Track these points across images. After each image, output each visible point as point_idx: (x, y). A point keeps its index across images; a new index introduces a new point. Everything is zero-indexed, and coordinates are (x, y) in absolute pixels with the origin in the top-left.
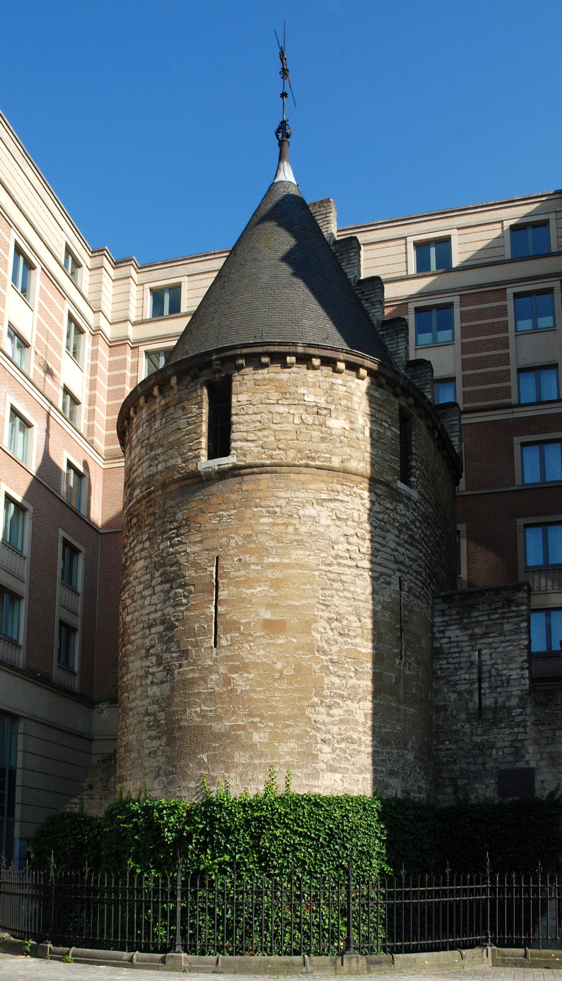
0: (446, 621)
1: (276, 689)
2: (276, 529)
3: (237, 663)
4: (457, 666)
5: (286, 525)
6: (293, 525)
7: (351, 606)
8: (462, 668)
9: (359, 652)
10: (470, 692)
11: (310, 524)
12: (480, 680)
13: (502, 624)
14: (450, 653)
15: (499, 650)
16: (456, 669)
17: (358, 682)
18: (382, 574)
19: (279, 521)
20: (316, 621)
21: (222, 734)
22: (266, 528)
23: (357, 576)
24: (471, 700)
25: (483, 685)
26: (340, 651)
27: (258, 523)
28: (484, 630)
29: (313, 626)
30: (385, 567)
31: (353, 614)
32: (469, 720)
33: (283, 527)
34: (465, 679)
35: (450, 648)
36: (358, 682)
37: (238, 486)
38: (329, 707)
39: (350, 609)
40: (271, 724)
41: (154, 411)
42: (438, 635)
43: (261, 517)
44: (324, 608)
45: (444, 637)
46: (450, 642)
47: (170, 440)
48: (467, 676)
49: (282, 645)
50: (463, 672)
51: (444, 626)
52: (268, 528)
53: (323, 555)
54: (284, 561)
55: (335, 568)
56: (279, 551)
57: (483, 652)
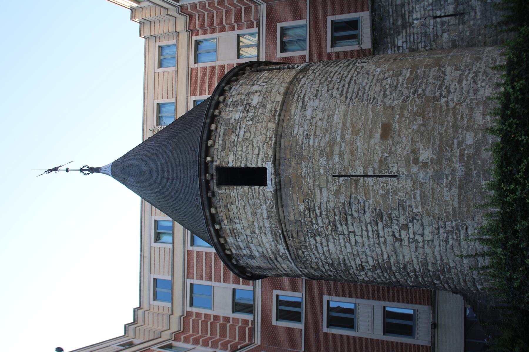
0: (391, 46)
1: (433, 129)
2: (318, 133)
3: (412, 158)
4: (423, 35)
5: (316, 126)
6: (317, 122)
7: (376, 84)
8: (426, 32)
9: (409, 78)
10: (443, 24)
11: (318, 112)
12: (435, 17)
13: (396, 5)
14: (414, 41)
15: (414, 6)
16: (425, 36)
17: (431, 77)
18: (356, 70)
19: (313, 132)
20: (385, 104)
21: (466, 168)
22: (317, 141)
23: (355, 83)
24: (449, 22)
25: (438, 15)
26: (407, 88)
27: (313, 146)
28: (400, 18)
29: (388, 106)
30: (351, 69)
31: (382, 82)
32: (464, 23)
33: (318, 128)
34: (433, 28)
35: (410, 41)
36: (431, 77)
37: (287, 162)
38: (449, 92)
39: (378, 84)
40: (460, 131)
41: (230, 231)
42: (401, 51)
43: (309, 145)
44: (376, 100)
45: (402, 47)
46: (406, 42)
47: (251, 215)
48: (431, 27)
49: (400, 126)
50: (428, 30)
51: (394, 47)
52: (317, 139)
53: (339, 102)
54: (340, 127)
55: (349, 95)
56: (333, 130)
57: (414, 17)
